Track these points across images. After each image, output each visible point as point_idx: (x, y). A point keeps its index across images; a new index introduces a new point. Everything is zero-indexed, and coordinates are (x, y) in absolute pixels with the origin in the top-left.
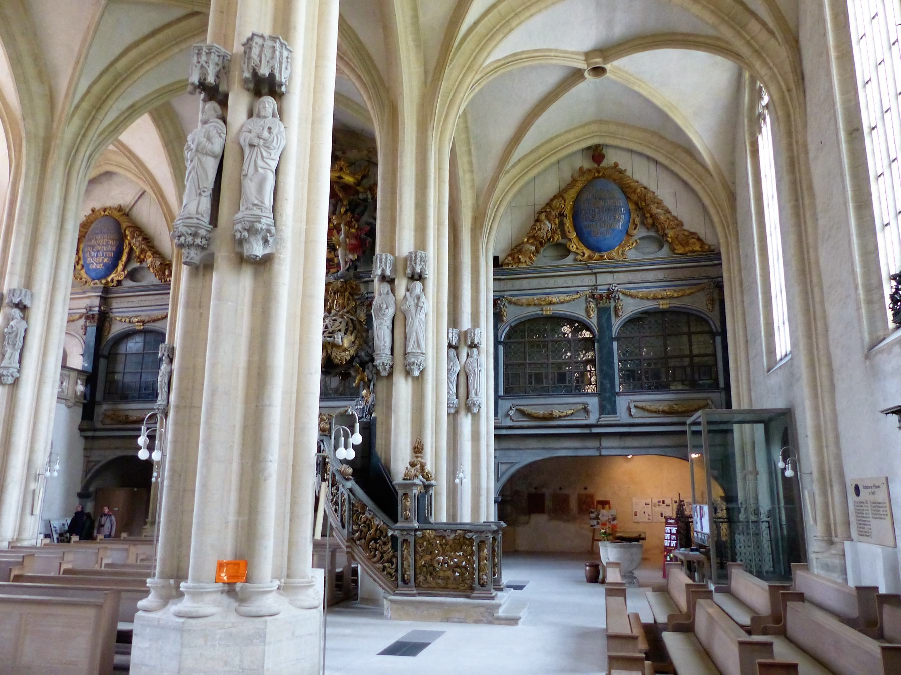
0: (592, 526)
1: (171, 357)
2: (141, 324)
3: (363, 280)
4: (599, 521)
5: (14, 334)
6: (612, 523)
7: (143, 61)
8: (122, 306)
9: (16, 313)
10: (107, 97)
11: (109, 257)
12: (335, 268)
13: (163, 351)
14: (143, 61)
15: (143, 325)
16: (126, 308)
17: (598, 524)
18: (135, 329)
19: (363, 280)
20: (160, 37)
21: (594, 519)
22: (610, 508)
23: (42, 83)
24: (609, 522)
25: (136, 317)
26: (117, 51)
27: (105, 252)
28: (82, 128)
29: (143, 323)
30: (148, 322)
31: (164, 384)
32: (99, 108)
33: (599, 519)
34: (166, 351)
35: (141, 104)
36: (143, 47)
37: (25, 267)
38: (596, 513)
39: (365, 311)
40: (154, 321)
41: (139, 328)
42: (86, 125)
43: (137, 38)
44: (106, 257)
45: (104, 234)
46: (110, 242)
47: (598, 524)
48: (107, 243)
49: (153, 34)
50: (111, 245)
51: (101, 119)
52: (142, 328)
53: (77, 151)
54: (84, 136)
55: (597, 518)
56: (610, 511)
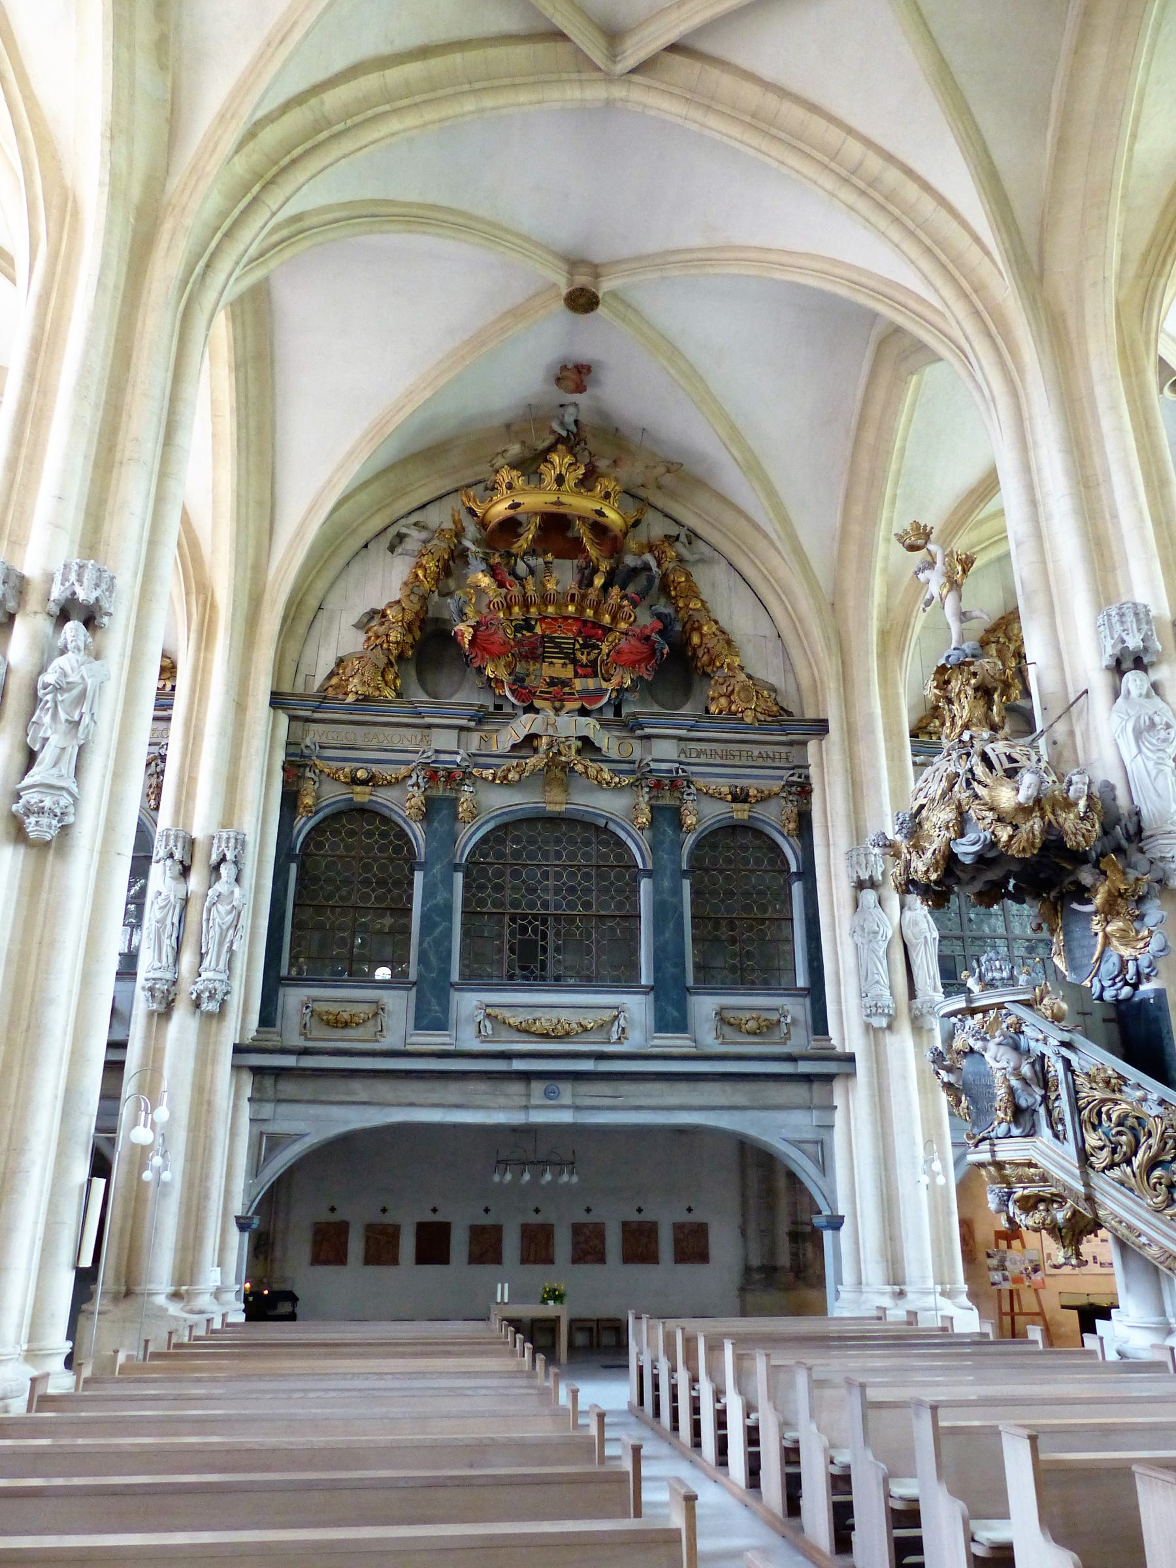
0: (993, 1284)
1: (187, 863)
3: (639, 732)
4: (1007, 1273)
5: (75, 692)
6: (1033, 1277)
7: (387, 107)
9: (73, 629)
10: (294, 162)
12: (575, 700)
13: (172, 843)
14: (387, 107)
17: (1005, 1279)
19: (639, 732)
20: (437, 64)
21: (996, 1269)
22: (1024, 1246)
23: (163, 67)
24: (1028, 1276)
26: (339, 63)
28: (224, 215)
31: (169, 926)
32: (272, 182)
33: (1004, 1268)
34: (180, 845)
35: (314, 221)
36: (394, 75)
37: (82, 516)
38: (998, 1257)
39: (647, 797)
42: (236, 212)
43: (386, 49)
47: (1005, 1279)
49: (423, 52)
51: (274, 208)
53: (208, 266)
54: (228, 235)
55: (1002, 1267)
56: (1025, 1252)
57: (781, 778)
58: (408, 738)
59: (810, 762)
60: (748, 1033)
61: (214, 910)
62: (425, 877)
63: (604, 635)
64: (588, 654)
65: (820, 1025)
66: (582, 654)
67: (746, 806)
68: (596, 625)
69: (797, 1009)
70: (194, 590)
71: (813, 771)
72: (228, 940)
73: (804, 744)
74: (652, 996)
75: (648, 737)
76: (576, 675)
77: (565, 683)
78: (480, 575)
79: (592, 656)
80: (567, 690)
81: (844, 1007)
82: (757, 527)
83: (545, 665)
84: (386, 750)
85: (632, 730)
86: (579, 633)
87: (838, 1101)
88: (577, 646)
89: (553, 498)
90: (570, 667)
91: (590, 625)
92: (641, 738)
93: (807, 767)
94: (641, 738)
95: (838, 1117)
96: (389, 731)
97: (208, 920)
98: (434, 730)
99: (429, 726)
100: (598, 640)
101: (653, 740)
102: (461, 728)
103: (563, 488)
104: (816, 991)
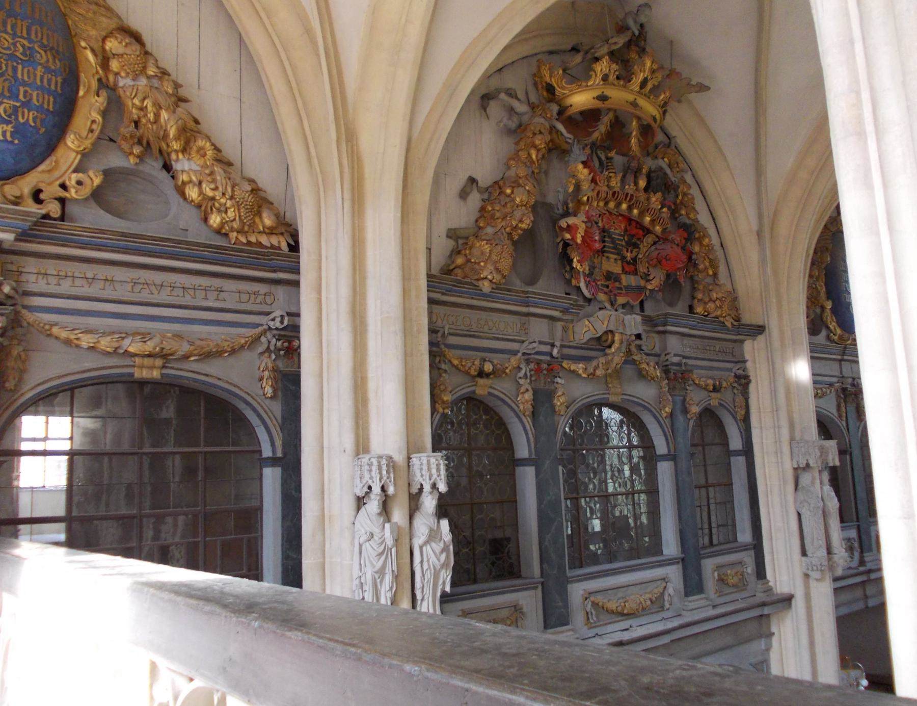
2: (159, 362)
8: (66, 287)
11: (39, 109)
15: (164, 367)
16: (69, 297)
18: (132, 375)
25: (145, 336)
27: (24, 84)
29: (164, 355)
30: (186, 357)
40: (207, 356)
41: (145, 374)
44: (27, 104)
45: (11, 14)
46: (42, 57)
48: (29, 54)
50: (47, 70)
52: (156, 374)
57: (730, 370)
58: (508, 325)
59: (747, 357)
60: (733, 586)
61: (427, 549)
62: (537, 474)
63: (644, 236)
64: (632, 252)
65: (761, 573)
66: (627, 251)
67: (718, 395)
68: (640, 225)
69: (748, 558)
70: (344, 137)
71: (749, 365)
72: (441, 582)
73: (742, 342)
74: (680, 566)
75: (664, 332)
76: (625, 272)
77: (617, 279)
78: (580, 166)
79: (634, 254)
80: (617, 284)
81: (775, 557)
82: (720, 150)
83: (604, 258)
84: (498, 339)
85: (656, 325)
86: (626, 230)
87: (774, 629)
88: (623, 243)
89: (631, 98)
90: (619, 262)
91: (634, 224)
92: (659, 332)
93: (745, 362)
94: (659, 332)
95: (775, 640)
96: (496, 316)
97: (422, 562)
98: (532, 318)
99: (528, 315)
100: (639, 239)
101: (667, 335)
102: (552, 318)
103: (643, 91)
104: (757, 547)
